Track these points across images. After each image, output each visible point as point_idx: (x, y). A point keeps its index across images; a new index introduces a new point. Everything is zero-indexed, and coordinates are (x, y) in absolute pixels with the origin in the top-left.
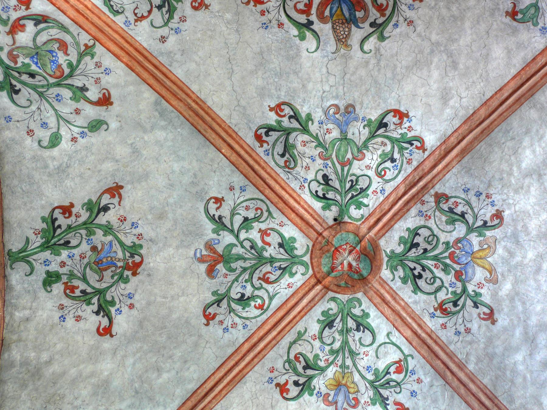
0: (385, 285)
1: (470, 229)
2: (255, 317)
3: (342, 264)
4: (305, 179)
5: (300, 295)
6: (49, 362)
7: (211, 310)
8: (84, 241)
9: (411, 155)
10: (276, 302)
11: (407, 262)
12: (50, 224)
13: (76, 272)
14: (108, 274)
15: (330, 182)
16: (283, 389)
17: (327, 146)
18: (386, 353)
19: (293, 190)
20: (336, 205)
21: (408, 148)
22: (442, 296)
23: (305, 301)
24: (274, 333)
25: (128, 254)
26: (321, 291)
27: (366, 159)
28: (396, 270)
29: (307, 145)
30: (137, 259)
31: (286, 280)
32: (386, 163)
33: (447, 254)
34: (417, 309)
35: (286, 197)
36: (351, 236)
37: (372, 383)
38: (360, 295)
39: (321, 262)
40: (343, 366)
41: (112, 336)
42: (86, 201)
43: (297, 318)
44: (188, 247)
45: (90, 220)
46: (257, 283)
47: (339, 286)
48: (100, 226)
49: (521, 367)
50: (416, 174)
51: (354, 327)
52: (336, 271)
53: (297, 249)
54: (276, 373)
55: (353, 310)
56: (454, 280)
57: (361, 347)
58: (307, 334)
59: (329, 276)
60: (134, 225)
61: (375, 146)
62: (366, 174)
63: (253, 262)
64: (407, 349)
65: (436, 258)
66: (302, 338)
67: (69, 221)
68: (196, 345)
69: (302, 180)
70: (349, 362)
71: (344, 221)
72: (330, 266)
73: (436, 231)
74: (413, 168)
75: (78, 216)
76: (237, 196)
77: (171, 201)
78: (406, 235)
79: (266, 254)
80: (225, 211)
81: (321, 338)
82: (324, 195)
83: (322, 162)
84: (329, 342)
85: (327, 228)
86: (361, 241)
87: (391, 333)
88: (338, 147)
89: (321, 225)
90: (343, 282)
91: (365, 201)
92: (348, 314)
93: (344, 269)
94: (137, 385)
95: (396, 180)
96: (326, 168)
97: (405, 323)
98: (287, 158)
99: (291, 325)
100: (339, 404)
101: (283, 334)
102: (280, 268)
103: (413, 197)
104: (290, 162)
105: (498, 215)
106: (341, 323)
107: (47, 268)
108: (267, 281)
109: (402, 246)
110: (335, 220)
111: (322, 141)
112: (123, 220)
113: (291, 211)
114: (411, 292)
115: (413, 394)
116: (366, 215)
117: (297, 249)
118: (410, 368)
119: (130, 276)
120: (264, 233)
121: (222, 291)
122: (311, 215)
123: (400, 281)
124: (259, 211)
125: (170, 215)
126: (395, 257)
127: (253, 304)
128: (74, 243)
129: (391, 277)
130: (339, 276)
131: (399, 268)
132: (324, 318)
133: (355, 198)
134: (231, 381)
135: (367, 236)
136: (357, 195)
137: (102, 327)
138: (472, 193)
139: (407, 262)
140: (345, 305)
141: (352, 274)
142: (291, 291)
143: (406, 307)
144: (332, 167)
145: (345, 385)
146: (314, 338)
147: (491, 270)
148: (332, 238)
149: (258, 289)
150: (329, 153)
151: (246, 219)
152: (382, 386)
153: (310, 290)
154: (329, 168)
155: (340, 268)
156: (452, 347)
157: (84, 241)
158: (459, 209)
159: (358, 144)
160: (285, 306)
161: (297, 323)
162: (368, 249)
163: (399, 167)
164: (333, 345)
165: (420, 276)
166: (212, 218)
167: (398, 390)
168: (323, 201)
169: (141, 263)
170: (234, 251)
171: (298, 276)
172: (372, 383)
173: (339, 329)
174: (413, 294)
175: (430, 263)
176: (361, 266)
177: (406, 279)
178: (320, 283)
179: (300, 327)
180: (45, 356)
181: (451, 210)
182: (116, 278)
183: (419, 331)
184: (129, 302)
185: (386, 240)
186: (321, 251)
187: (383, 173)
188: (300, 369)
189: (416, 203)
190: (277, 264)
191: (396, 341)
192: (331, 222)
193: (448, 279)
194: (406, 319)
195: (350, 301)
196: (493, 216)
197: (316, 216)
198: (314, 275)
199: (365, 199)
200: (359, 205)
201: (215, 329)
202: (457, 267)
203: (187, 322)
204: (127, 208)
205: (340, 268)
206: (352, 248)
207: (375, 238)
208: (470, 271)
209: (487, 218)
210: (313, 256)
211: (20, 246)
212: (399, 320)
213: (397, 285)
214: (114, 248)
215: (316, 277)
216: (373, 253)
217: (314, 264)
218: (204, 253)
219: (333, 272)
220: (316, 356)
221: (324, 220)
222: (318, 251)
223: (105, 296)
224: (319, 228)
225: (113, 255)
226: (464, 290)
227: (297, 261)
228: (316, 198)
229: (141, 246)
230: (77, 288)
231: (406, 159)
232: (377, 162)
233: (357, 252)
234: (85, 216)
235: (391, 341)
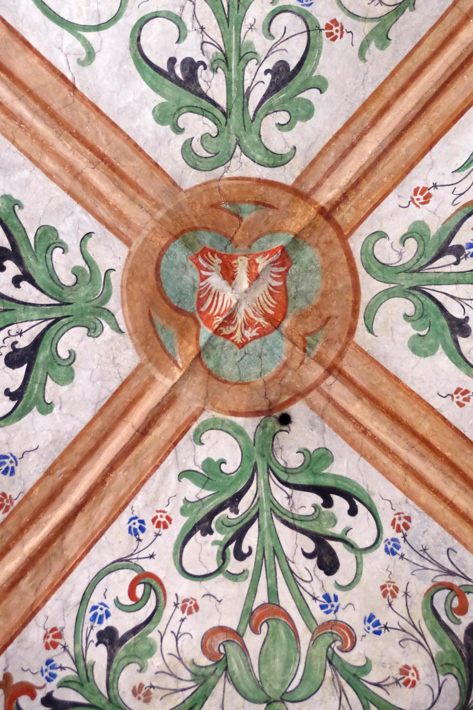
0: (110, 218)
4: (394, 553)
9: (49, 662)
11: (44, 299)
15: (310, 546)
17: (329, 673)
19: (430, 513)
20: (286, 470)
21: (60, 686)
26: (318, 185)
27: (198, 634)
28: (76, 271)
29: (396, 673)
32: (131, 626)
39: (324, 277)
43: (391, 89)
50: (30, 599)
52: (274, 252)
53: (406, 317)
55: (211, 128)
57: (177, 11)
58: (358, 40)
59: (296, 236)
61: (171, 683)
62: (195, 584)
66: (374, 24)
69: (404, 549)
71: (257, 420)
72: (294, 269)
74: (40, 616)
82: (328, 503)
83: (342, 616)
85: (309, 390)
86: (199, 356)
87: (81, 63)
88: (293, 669)
89: (330, 399)
90: (246, 217)
92: (226, 115)
93: (246, 260)
95: (94, 571)
96: (327, 597)
97: (37, 99)
98: (458, 622)
99: (412, 66)
101: (440, 35)
104: (450, 611)
106: (247, 84)
109: (63, 353)
111: (348, 689)
113: (434, 441)
114: (25, 203)
117: (406, 317)
122: (365, 431)
123: (61, 237)
126: (82, 315)
130: (261, 235)
132: (305, 95)
133: (225, 497)
135: (178, 375)
136: (221, 508)
139: (44, 299)
140: (238, 143)
141: (219, 248)
144: (309, 599)
148: (291, 358)
150: (320, 650)
154: (319, 594)
155: (262, 262)
159: (229, 687)
160: (436, 128)
161: (393, 74)
162: (172, 330)
163: (89, 615)
164: (271, 8)
168: (329, 482)
173: (252, 65)
174: (16, 196)
177: (44, 245)
178: (322, 211)
185: (117, 365)
186: (325, 314)
187: (140, 590)
189: (26, 497)
191: (61, 36)
194: (35, 113)
197: (349, 427)
199: (192, 498)
205: (262, 262)
206: (226, 331)
207: (154, 371)
210: (350, 297)
212: (56, 106)
215: (338, 229)
216: (157, 319)
217: (344, 270)
219: (283, 249)
221: (322, 417)
222: (335, 312)
227: (403, 276)
228: (354, 491)
231: (65, 647)
232: (161, 626)
233: (208, 321)
235: (79, 37)
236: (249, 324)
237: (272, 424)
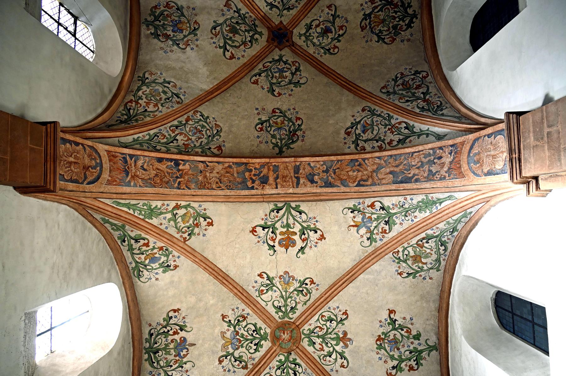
1: (232, 354)
2: (325, 312)
3: (287, 334)
5: (306, 320)
6: (417, 301)
7: (344, 317)
8: (403, 353)
10: (316, 317)
12: (419, 362)
13: (406, 339)
14: (392, 337)
15: (293, 372)
16: (312, 282)
18: (268, 297)
22: (244, 324)
23: (303, 318)
24: (316, 304)
25: (383, 345)
28: (264, 333)
30: (378, 343)
31: (312, 327)
33: (242, 342)
34: (255, 316)
35: (312, 365)
36: (283, 346)
37: (274, 286)
38: (280, 320)
40: (286, 292)
41: (389, 309)
42: (403, 372)
43: (306, 310)
44: (355, 347)
45: (400, 362)
46: (325, 327)
47: (289, 324)
48: (396, 359)
49: (211, 298)
51: (282, 308)
54: (316, 288)
56: (239, 331)
60: (380, 359)
63: (326, 337)
64: (259, 299)
65: (247, 340)
67: (410, 363)
68: (351, 302)
70: (284, 293)
73: (247, 352)
75: (406, 365)
76: (334, 367)
77: (364, 369)
78: (260, 349)
79: (321, 340)
80: (340, 361)
81: (296, 303)
82: (296, 366)
84: (292, 301)
91: (278, 363)
94: (377, 288)
100: (288, 276)
102: (315, 333)
103: (257, 366)
105: (220, 362)
107: (419, 342)
108: (320, 328)
110: (291, 354)
112: (385, 362)
115: (256, 282)
116: (277, 356)
118: (257, 292)
119: (381, 335)
120: (322, 349)
121: (340, 325)
124: (324, 359)
125: (364, 362)
127: (326, 318)
128: (408, 353)
129: (266, 330)
131: (262, 334)
134: (335, 286)
137: (393, 314)
138: (232, 371)
142: (310, 322)
143: (260, 317)
145: (285, 284)
146: (299, 303)
147: (223, 337)
149: (324, 325)
151: (330, 356)
152: (269, 285)
153: (301, 323)
155: (288, 332)
156: (240, 302)
157: (403, 353)
158: (238, 362)
165: (254, 331)
166: (345, 358)
167: (263, 283)
169: (377, 340)
170: (335, 342)
171: (306, 329)
172: (274, 286)
175: (250, 337)
176: (279, 334)
179: (305, 307)
180: (419, 303)
181: (241, 362)
182: (388, 335)
183: (254, 307)
184: (381, 324)
188: (305, 290)
190: (316, 335)
192: (292, 352)
193: (242, 331)
195: (284, 318)
196: (223, 361)
198: (299, 329)
200: (280, 361)
201: (343, 308)
202: (238, 337)
203: (355, 312)
204: (383, 367)
205: (288, 332)
208: (232, 336)
209: (225, 360)
211: (432, 353)
213: (263, 326)
214: (389, 348)
218: (348, 343)
220: (298, 295)
223: (393, 327)
224: (298, 350)
225: (390, 346)
226: (235, 327)
229: (377, 348)
230: (405, 332)
234: (403, 365)
236: (286, 340)
237: (289, 354)
